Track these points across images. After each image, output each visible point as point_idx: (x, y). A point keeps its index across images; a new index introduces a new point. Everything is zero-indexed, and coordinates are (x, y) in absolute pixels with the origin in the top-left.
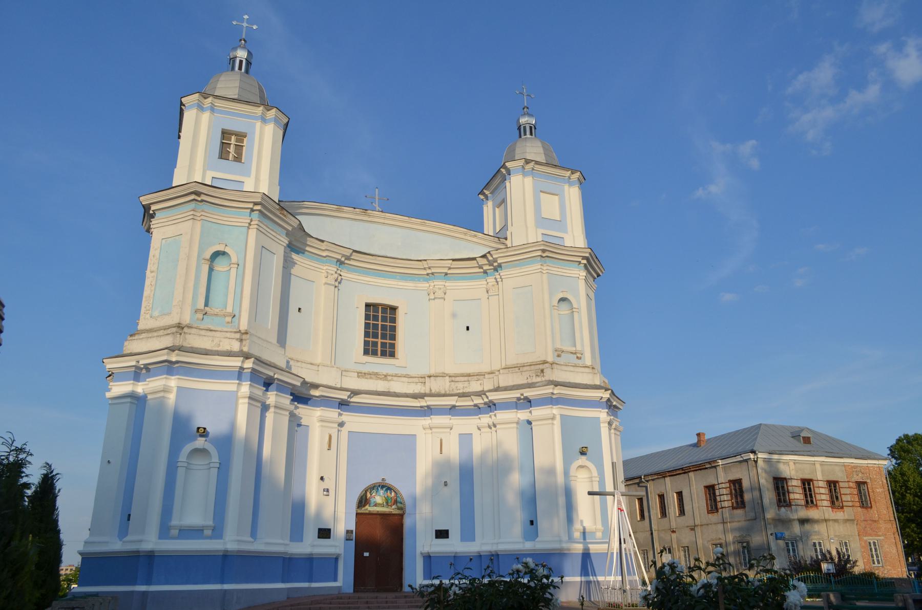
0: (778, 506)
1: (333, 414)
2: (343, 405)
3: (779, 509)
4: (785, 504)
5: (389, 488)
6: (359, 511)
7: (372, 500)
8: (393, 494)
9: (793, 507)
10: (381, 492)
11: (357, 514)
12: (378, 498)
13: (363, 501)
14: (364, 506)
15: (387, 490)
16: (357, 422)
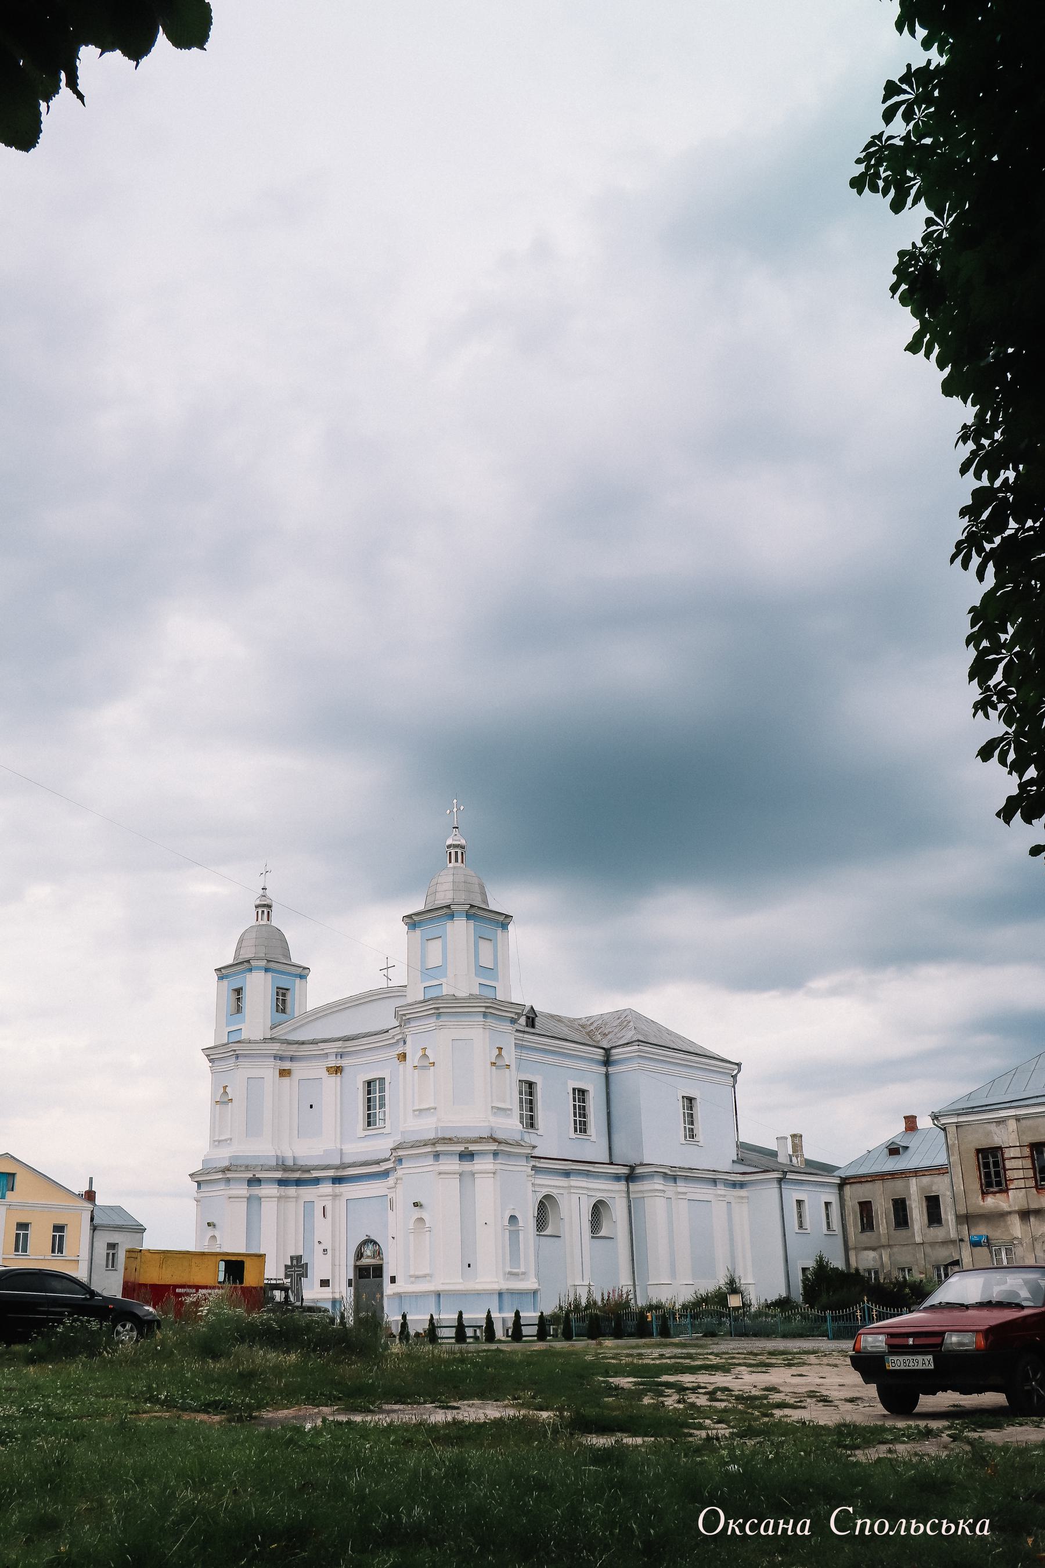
0: (983, 1193)
1: (326, 1188)
2: (337, 1180)
3: (983, 1199)
4: (995, 1189)
5: (375, 1243)
6: (358, 1263)
7: (365, 1254)
8: (377, 1247)
9: (1011, 1192)
10: (370, 1246)
11: (356, 1267)
12: (368, 1251)
13: (359, 1255)
14: (360, 1259)
15: (373, 1244)
16: (348, 1190)
